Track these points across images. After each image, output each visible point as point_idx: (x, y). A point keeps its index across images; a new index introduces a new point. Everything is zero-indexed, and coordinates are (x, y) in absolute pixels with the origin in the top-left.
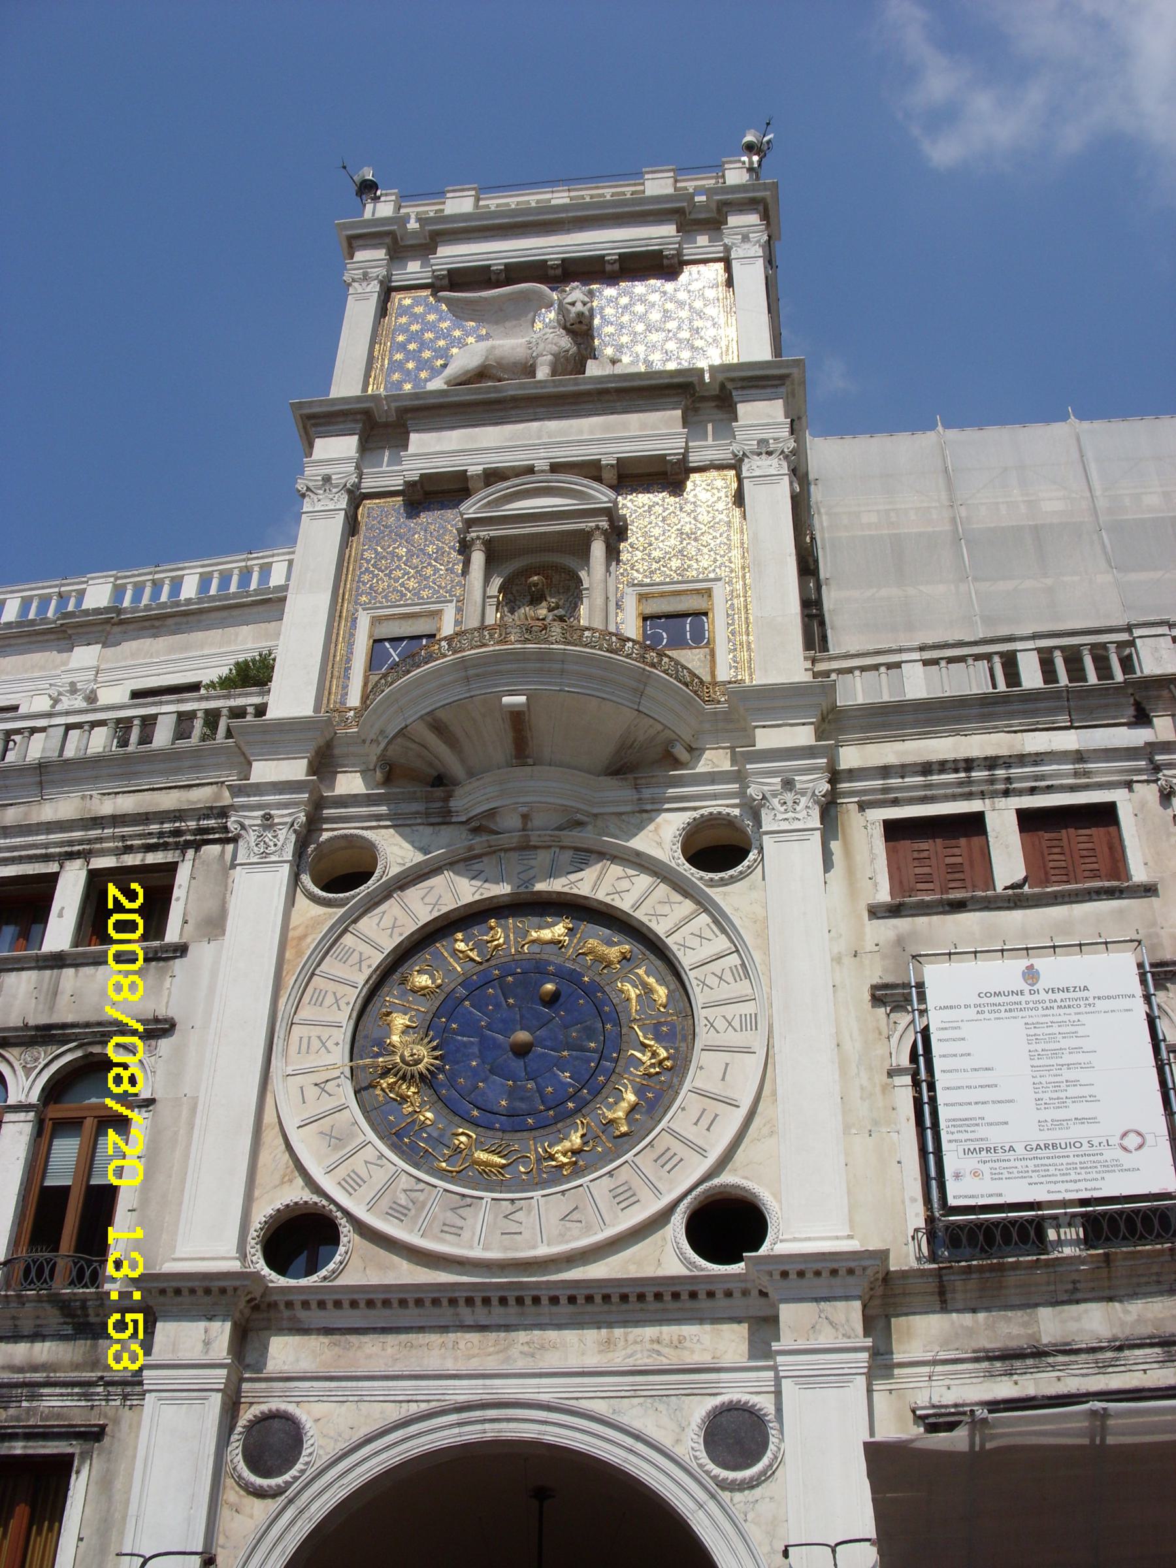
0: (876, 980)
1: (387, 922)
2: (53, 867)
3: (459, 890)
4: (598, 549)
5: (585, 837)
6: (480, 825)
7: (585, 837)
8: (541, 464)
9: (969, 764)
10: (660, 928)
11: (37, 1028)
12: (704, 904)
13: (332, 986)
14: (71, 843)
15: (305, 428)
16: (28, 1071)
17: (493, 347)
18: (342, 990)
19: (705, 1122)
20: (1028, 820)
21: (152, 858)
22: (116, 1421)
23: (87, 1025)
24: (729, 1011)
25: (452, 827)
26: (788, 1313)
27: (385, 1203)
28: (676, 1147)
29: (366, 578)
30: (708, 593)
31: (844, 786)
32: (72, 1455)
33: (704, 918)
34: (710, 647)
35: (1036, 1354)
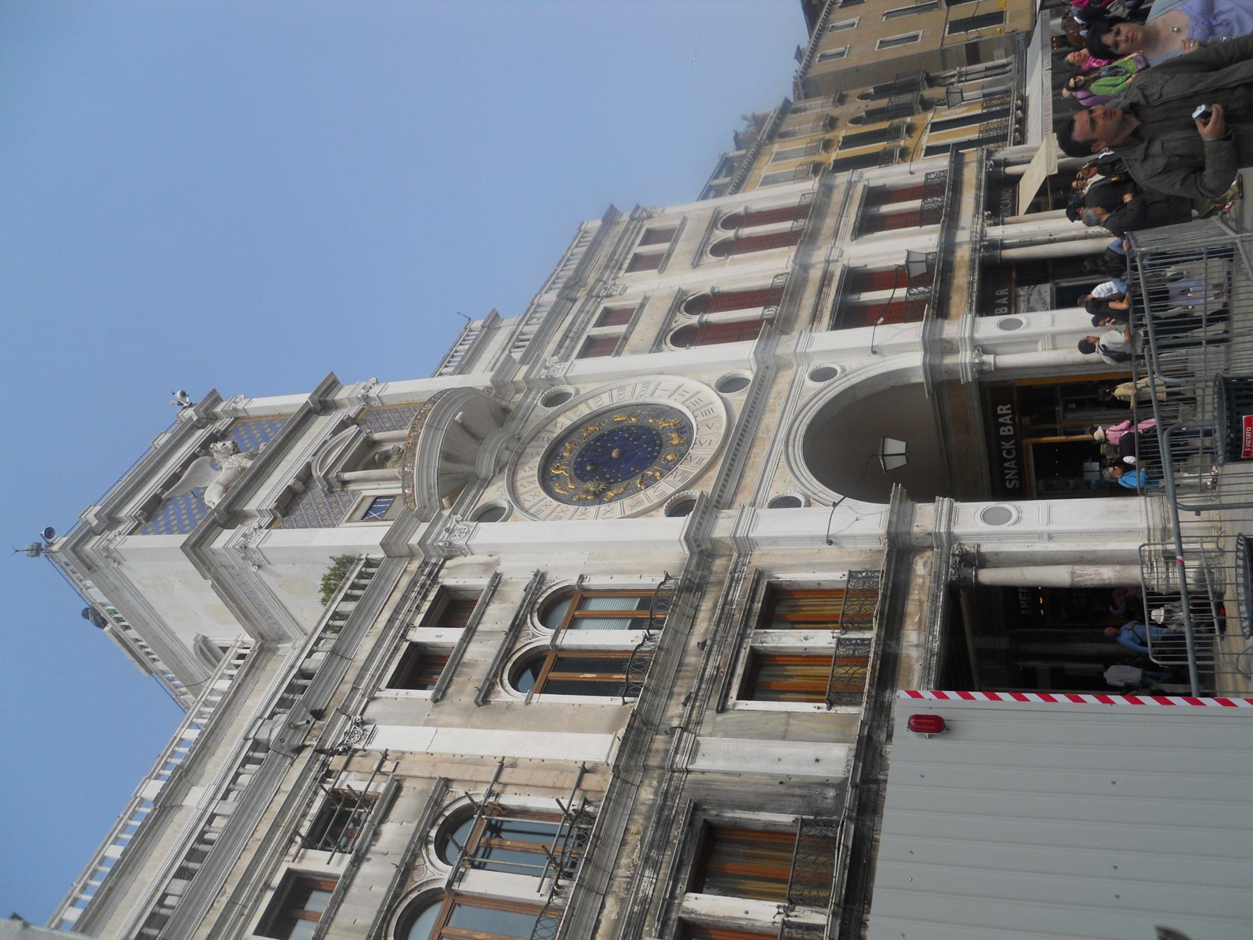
2: (405, 645)
11: (510, 630)
14: (395, 637)
15: (196, 554)
16: (534, 636)
21: (431, 597)
23: (521, 606)
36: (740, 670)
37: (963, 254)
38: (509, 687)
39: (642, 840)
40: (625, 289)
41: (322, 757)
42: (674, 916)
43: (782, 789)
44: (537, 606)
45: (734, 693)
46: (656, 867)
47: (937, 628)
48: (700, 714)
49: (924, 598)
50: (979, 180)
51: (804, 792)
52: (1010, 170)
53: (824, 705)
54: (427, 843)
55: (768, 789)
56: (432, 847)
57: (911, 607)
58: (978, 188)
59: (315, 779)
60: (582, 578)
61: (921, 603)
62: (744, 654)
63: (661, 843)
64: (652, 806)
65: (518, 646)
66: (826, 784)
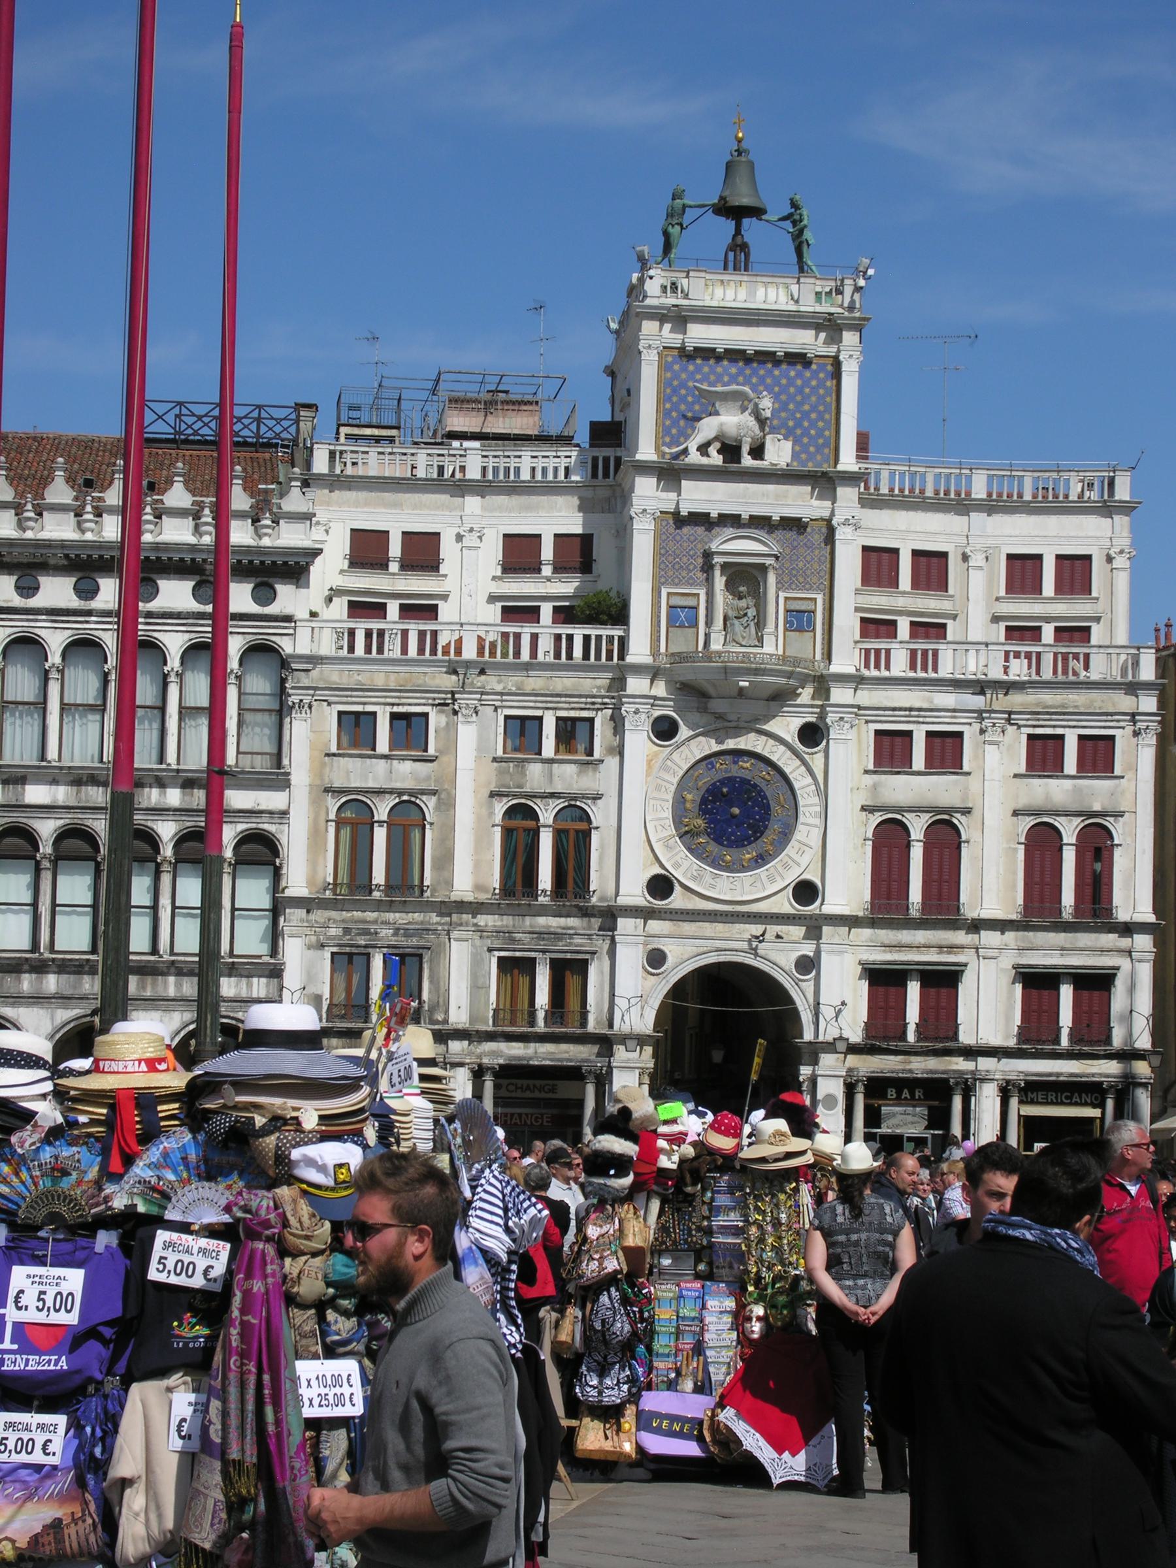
1: (683, 756)
2: (539, 713)
3: (711, 746)
6: (720, 717)
8: (745, 516)
9: (911, 709)
10: (787, 770)
12: (804, 763)
13: (664, 784)
14: (546, 702)
17: (721, 425)
18: (668, 785)
21: (585, 714)
26: (825, 928)
28: (790, 862)
29: (662, 566)
33: (803, 768)
35: (900, 947)
36: (518, 954)
40: (996, 743)
42: (370, 950)
43: (442, 990)
45: (503, 954)
46: (395, 934)
47: (548, 1063)
50: (1093, 1075)
51: (441, 1002)
52: (1110, 1104)
54: (399, 797)
56: (397, 800)
57: (564, 1047)
58: (1072, 1075)
59: (434, 699)
60: (597, 828)
62: (533, 955)
63: (408, 934)
65: (538, 801)
66: (447, 1012)
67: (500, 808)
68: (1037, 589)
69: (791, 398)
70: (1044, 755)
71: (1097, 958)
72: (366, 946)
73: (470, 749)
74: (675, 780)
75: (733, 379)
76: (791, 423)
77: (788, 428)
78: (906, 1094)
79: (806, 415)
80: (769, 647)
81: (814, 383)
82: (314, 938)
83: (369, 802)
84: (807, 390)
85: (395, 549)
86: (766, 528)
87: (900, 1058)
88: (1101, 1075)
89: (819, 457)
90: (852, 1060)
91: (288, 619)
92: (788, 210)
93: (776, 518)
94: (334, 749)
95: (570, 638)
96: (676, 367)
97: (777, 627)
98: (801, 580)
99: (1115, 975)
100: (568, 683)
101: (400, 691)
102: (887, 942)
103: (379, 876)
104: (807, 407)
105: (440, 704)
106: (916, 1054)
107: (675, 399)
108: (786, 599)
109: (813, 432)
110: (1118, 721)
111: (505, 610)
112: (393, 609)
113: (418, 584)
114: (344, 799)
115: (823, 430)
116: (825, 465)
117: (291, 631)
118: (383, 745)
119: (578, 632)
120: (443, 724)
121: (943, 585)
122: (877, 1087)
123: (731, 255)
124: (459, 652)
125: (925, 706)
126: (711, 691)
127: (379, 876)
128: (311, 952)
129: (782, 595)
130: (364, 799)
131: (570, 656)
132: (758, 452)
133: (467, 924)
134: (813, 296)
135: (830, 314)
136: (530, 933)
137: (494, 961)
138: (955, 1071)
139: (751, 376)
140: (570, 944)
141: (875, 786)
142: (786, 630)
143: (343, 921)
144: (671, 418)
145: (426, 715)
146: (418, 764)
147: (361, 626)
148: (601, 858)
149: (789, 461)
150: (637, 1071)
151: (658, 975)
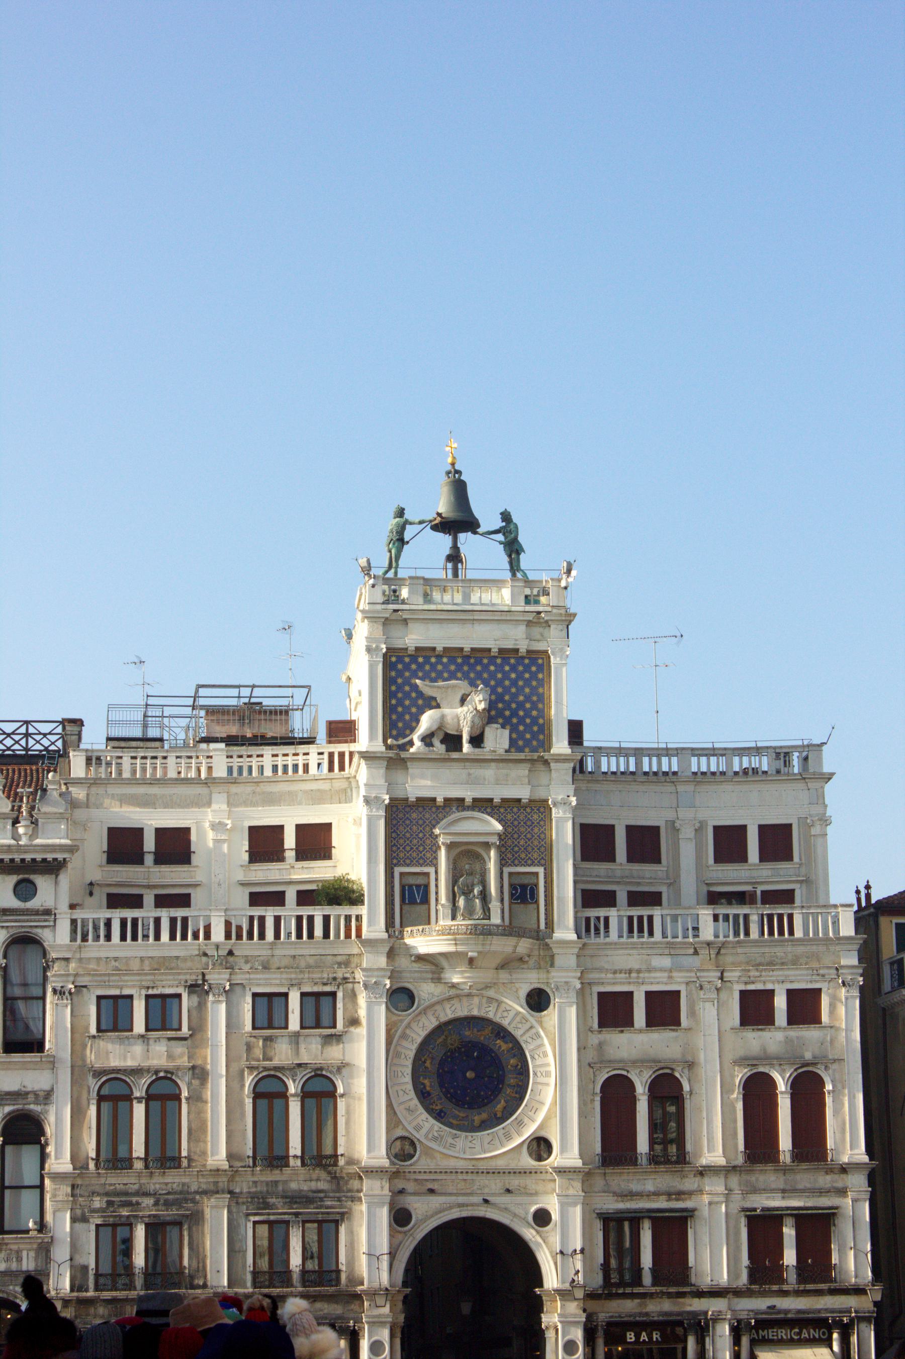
0: (591, 1060)
4: (493, 853)
5: (491, 993)
6: (454, 986)
7: (491, 993)
8: (468, 800)
9: (630, 971)
10: (517, 1034)
13: (403, 1051)
14: (291, 979)
16: (294, 1081)
17: (443, 717)
18: (407, 1052)
19: (533, 1111)
20: (648, 994)
21: (328, 989)
22: (350, 1209)
24: (542, 1069)
25: (443, 985)
27: (430, 1136)
29: (394, 848)
30: (537, 874)
31: (586, 976)
32: (338, 1221)
34: (537, 902)
36: (272, 1218)
37: (696, 1305)
38: (256, 1079)
39: (169, 1193)
41: (200, 977)
44: (319, 1072)
45: (257, 1218)
46: (156, 1204)
48: (243, 1203)
49: (326, 1311)
50: (819, 1311)
51: (201, 1268)
53: (252, 1269)
55: (201, 1249)
56: (154, 1077)
58: (799, 1311)
60: (342, 1096)
61: (321, 1310)
62: (286, 1217)
64: (188, 1193)
67: (249, 1080)
68: (742, 857)
69: (507, 690)
70: (755, 1009)
71: (815, 1199)
72: (128, 1217)
73: (222, 1024)
74: (414, 1047)
75: (452, 676)
76: (507, 713)
77: (504, 717)
78: (644, 1337)
79: (521, 705)
80: (496, 919)
81: (527, 676)
82: (79, 1212)
83: (128, 1080)
84: (521, 683)
85: (149, 844)
86: (489, 810)
87: (637, 1301)
88: (826, 1310)
89: (535, 743)
90: (593, 1305)
91: (47, 912)
92: (499, 524)
93: (497, 800)
94: (93, 1030)
95: (311, 919)
96: (400, 666)
97: (502, 901)
98: (523, 856)
99: (834, 1214)
100: (311, 961)
101: (154, 974)
102: (618, 1191)
103: (139, 1150)
104: (521, 698)
105: (191, 986)
106: (651, 1295)
107: (400, 695)
108: (511, 874)
109: (528, 721)
110: (823, 976)
111: (252, 895)
112: (149, 899)
113: (172, 876)
114: (104, 1079)
115: (537, 718)
116: (541, 750)
117: (52, 923)
118: (139, 1026)
119: (318, 912)
120: (196, 1004)
121: (656, 859)
122: (615, 1330)
123: (450, 565)
124: (208, 936)
125: (644, 967)
126: (444, 963)
127: (139, 1150)
128: (78, 1225)
129: (506, 870)
130: (124, 1077)
131: (311, 935)
132: (477, 740)
133: (223, 1192)
134: (523, 598)
135: (539, 613)
136: (283, 1197)
137: (250, 1225)
138: (689, 1313)
139: (468, 672)
140: (321, 1207)
141: (601, 1045)
142: (511, 904)
143: (107, 1194)
144: (396, 712)
145: (179, 996)
146: (173, 1043)
147: (117, 915)
148: (348, 1123)
149: (507, 746)
150: (388, 1326)
151: (405, 1232)
